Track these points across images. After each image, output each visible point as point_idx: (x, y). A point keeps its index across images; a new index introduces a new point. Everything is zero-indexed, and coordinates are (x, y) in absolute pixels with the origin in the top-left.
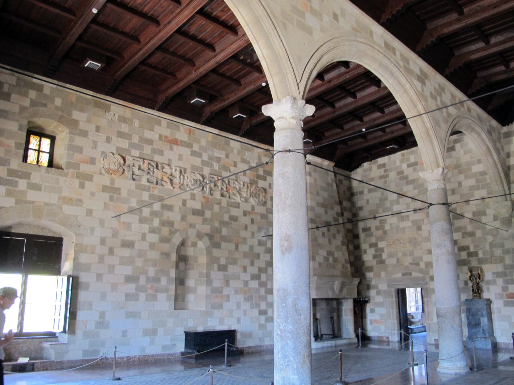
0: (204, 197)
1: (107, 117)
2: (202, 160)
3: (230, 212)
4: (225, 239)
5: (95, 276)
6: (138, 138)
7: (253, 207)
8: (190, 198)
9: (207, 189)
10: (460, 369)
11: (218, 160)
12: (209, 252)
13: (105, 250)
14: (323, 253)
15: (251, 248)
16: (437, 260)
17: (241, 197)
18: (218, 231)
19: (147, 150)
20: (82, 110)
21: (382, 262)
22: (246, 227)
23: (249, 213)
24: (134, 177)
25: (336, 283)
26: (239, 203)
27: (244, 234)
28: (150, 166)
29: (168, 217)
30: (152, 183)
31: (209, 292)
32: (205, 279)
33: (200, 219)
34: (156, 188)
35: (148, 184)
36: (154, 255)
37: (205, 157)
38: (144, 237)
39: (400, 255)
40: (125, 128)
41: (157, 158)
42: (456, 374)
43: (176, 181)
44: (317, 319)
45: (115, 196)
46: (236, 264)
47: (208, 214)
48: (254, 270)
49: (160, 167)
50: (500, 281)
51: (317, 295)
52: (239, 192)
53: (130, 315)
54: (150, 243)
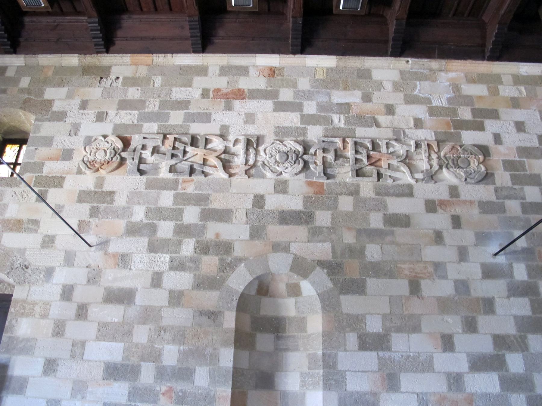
0: (310, 184)
2: (302, 116)
3: (385, 207)
4: (377, 270)
6: (158, 104)
7: (454, 191)
8: (273, 191)
9: (316, 169)
11: (344, 108)
12: (329, 304)
13: (71, 309)
15: (462, 286)
17: (412, 169)
18: (356, 252)
19: (176, 118)
20: (61, 84)
22: (438, 237)
23: (443, 203)
24: (142, 167)
26: (410, 187)
27: (432, 253)
29: (217, 235)
32: (321, 371)
33: (301, 231)
34: (192, 181)
35: (171, 176)
36: (178, 317)
37: (310, 108)
38: (157, 280)
40: (133, 93)
41: (197, 129)
43: (239, 161)
45: (102, 206)
46: (416, 329)
47: (323, 218)
48: (483, 344)
49: (202, 143)
52: (407, 160)
54: (171, 292)
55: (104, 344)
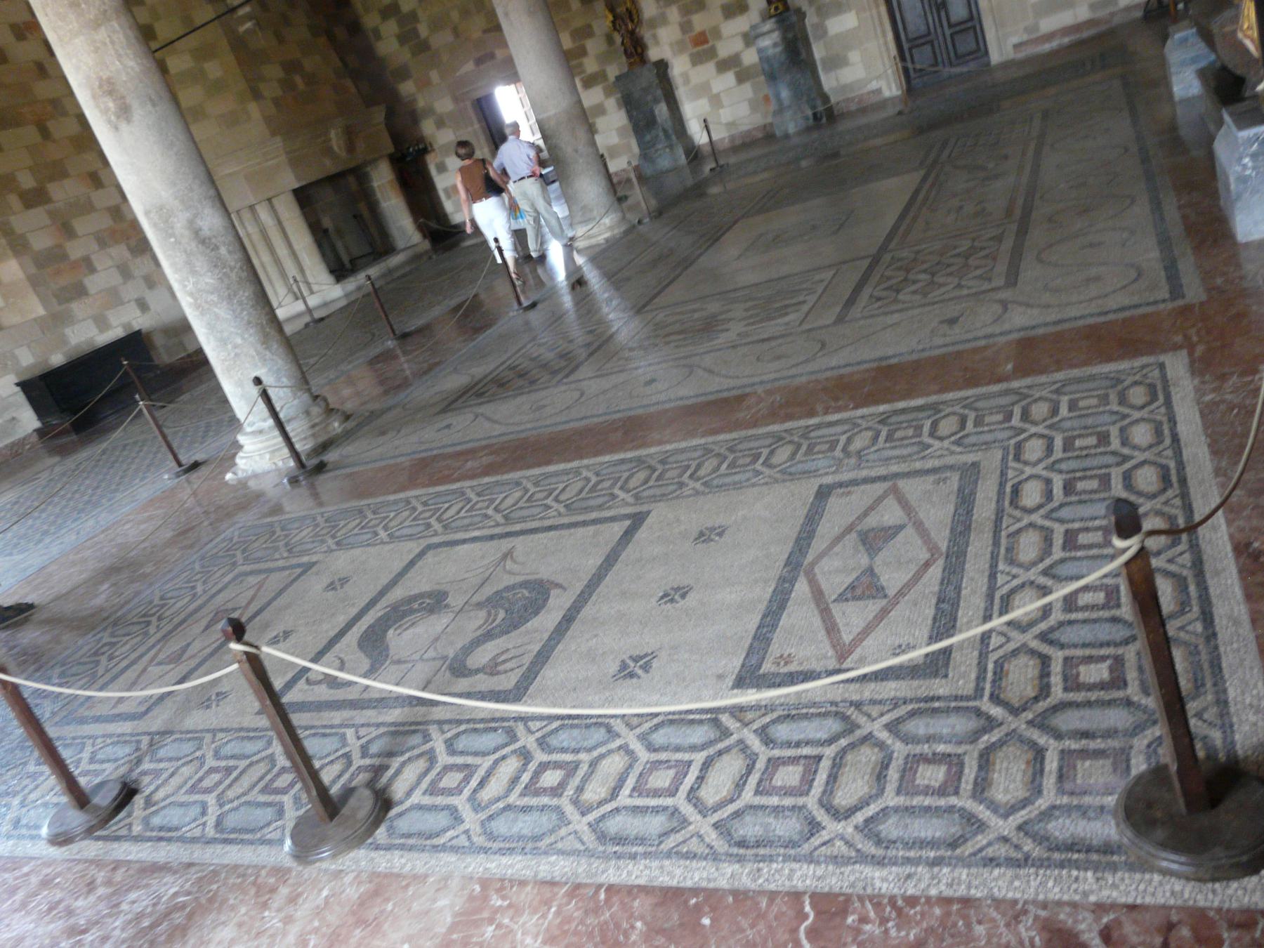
10: (611, 228)
14: (273, 71)
16: (506, 14)
21: (422, 47)
25: (333, 134)
31: (33, 270)
39: (455, 15)
42: (607, 240)
44: (326, 231)
46: (64, 174)
50: (674, 14)
51: (298, 178)
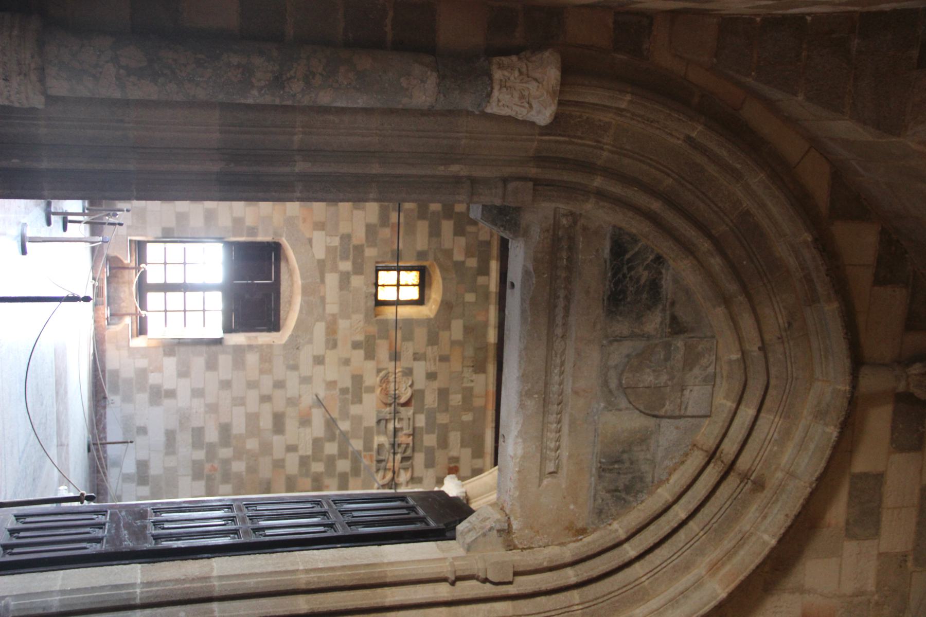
1: (465, 369)
5: (229, 377)
6: (444, 422)
24: (383, 422)
28: (403, 446)
30: (378, 453)
35: (375, 446)
38: (291, 448)
40: (456, 399)
41: (419, 459)
45: (349, 396)
53: (170, 437)
55: (243, 420)
